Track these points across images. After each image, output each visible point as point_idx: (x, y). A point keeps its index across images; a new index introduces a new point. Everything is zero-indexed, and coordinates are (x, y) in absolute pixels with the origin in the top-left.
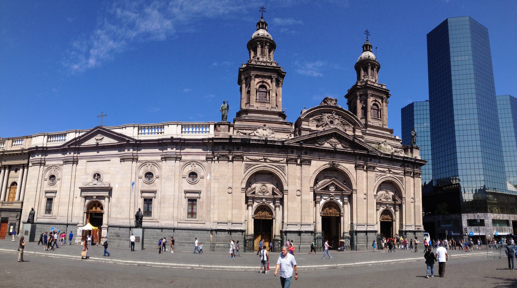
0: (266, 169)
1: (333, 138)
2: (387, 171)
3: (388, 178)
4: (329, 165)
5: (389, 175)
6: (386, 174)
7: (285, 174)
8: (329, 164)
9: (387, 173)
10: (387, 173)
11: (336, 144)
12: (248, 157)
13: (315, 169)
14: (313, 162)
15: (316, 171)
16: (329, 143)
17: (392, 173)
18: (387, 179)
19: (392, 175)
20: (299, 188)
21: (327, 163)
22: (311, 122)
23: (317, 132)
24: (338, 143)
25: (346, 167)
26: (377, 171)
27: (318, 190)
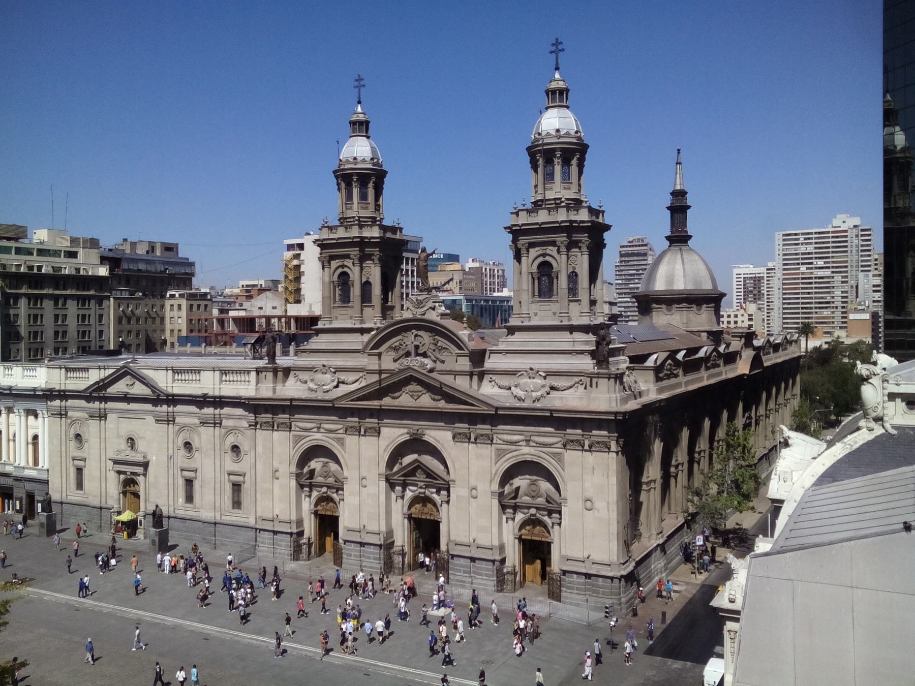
0: (320, 443)
1: (412, 383)
2: (523, 441)
3: (523, 456)
4: (408, 435)
5: (526, 450)
6: (520, 448)
7: (345, 453)
8: (407, 433)
9: (521, 446)
10: (521, 446)
11: (420, 394)
12: (298, 424)
13: (387, 443)
14: (384, 430)
15: (388, 445)
16: (407, 393)
17: (535, 444)
18: (521, 459)
19: (532, 450)
20: (363, 474)
21: (406, 430)
22: (385, 353)
23: (392, 373)
24: (423, 392)
25: (437, 438)
26: (499, 442)
27: (396, 477)
